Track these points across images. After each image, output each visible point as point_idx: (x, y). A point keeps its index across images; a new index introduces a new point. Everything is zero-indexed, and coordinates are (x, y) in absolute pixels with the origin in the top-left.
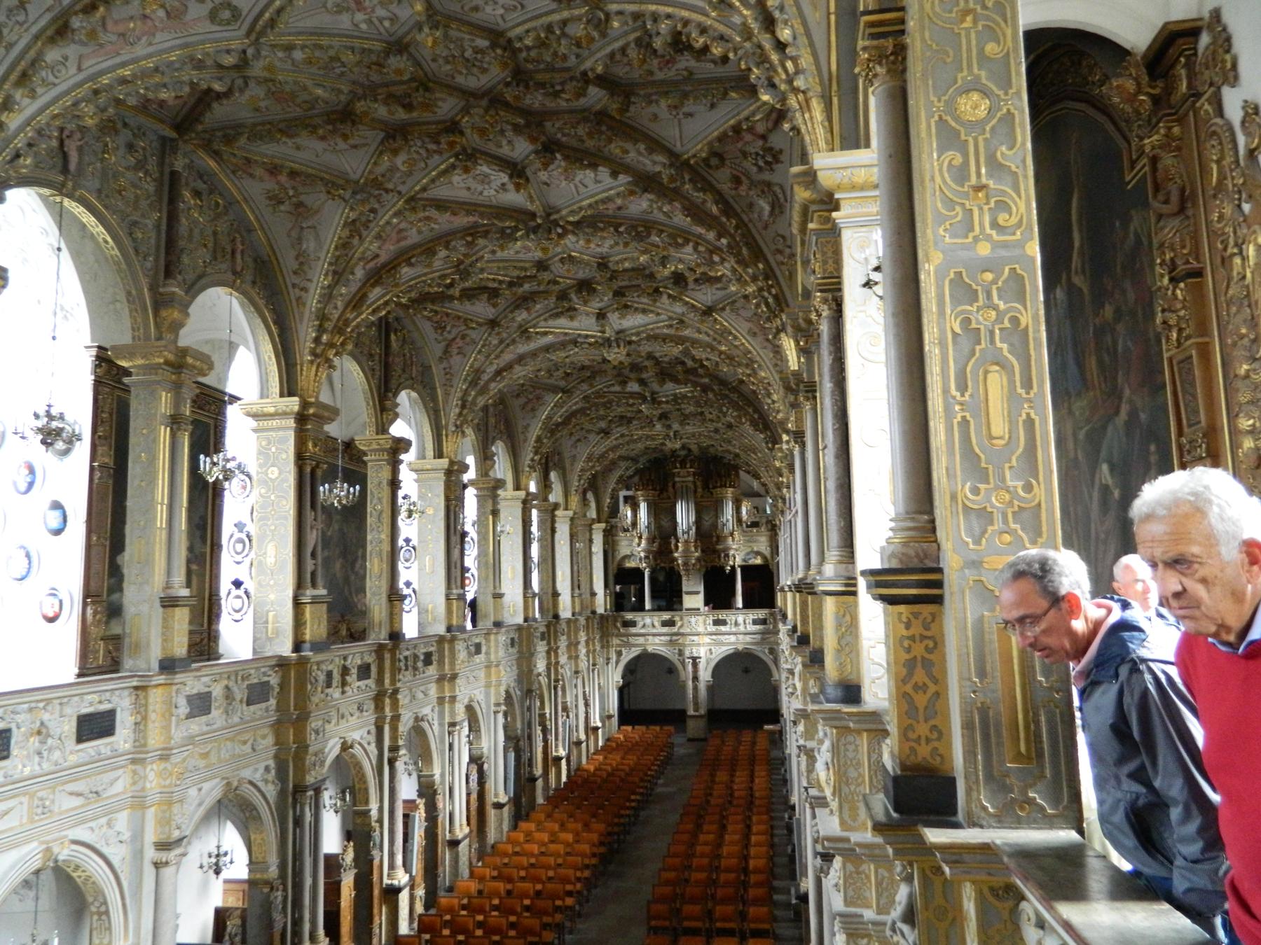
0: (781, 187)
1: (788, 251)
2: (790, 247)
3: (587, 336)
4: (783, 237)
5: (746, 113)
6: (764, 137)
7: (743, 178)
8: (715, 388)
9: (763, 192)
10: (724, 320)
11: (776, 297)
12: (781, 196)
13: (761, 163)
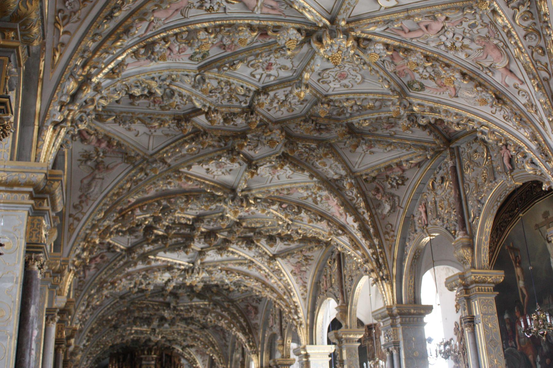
0: (399, 198)
1: (392, 233)
2: (393, 231)
3: (180, 265)
4: (391, 225)
5: (406, 158)
6: (404, 171)
7: (381, 189)
8: (226, 304)
9: (389, 199)
10: (280, 263)
11: (383, 258)
12: (397, 203)
13: (394, 184)
